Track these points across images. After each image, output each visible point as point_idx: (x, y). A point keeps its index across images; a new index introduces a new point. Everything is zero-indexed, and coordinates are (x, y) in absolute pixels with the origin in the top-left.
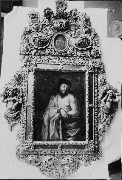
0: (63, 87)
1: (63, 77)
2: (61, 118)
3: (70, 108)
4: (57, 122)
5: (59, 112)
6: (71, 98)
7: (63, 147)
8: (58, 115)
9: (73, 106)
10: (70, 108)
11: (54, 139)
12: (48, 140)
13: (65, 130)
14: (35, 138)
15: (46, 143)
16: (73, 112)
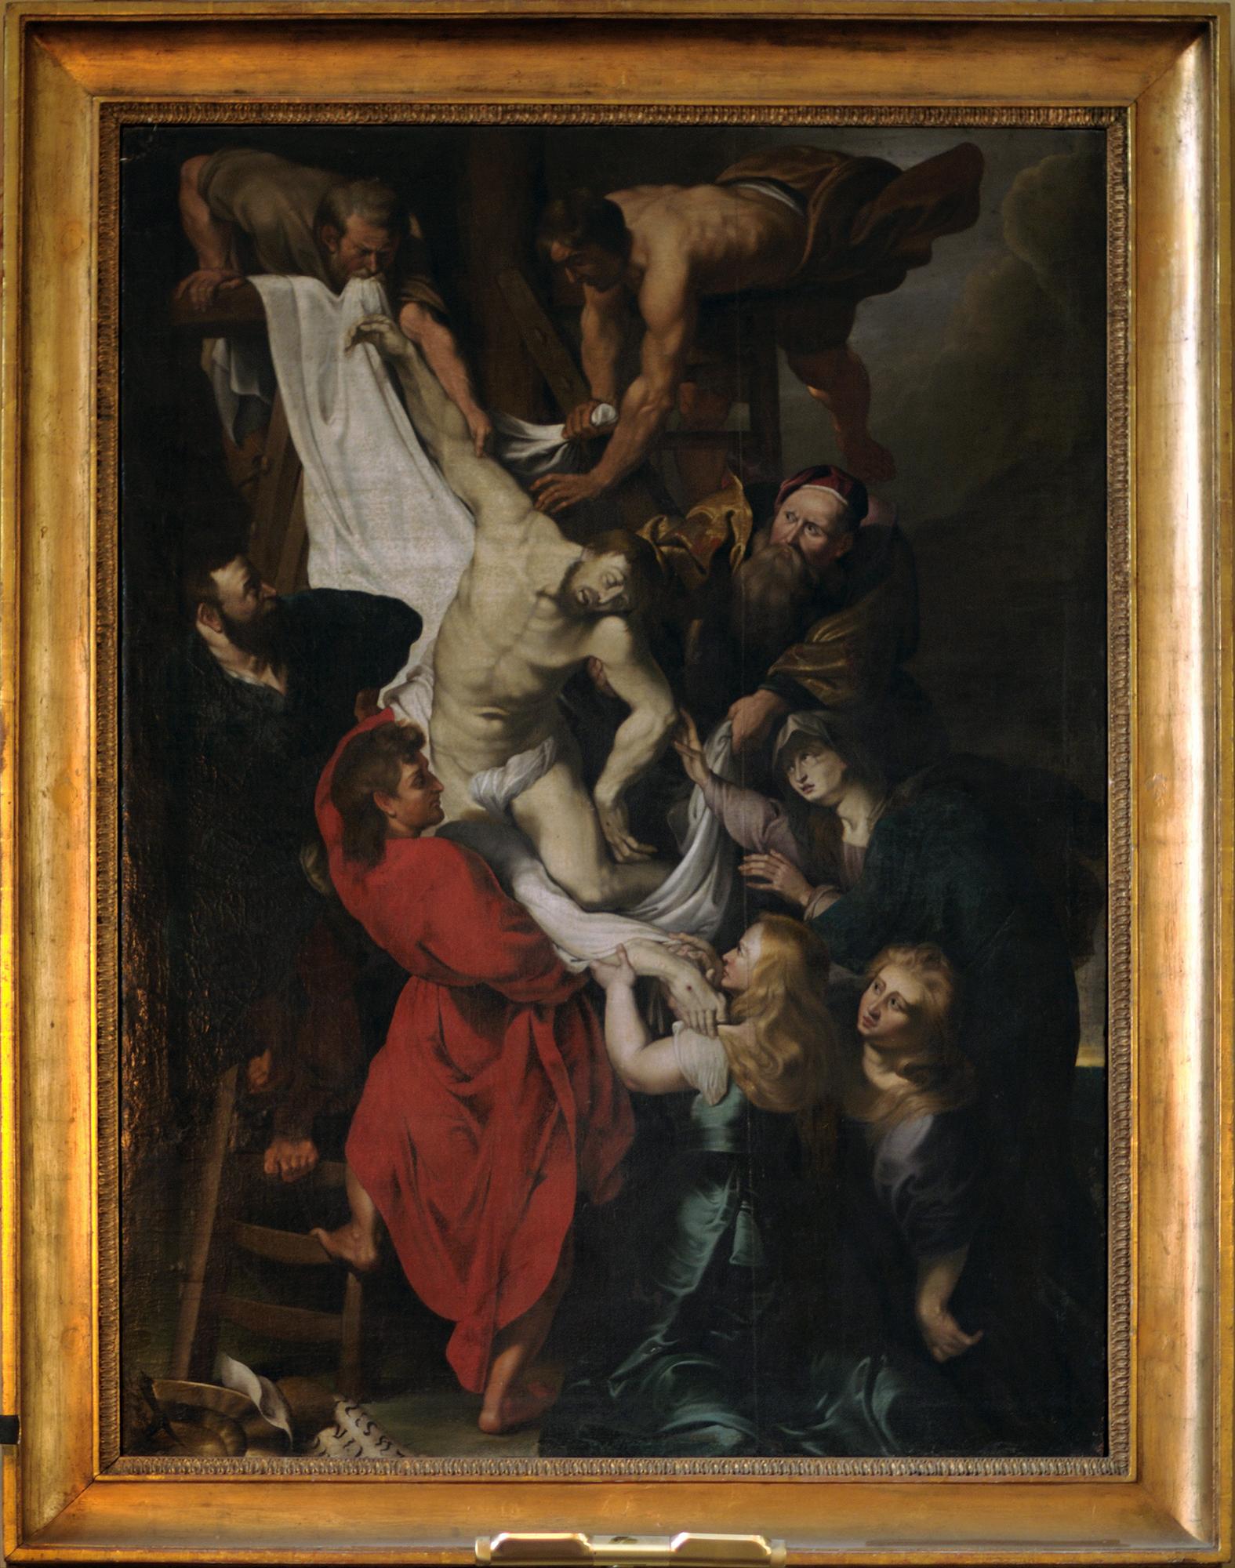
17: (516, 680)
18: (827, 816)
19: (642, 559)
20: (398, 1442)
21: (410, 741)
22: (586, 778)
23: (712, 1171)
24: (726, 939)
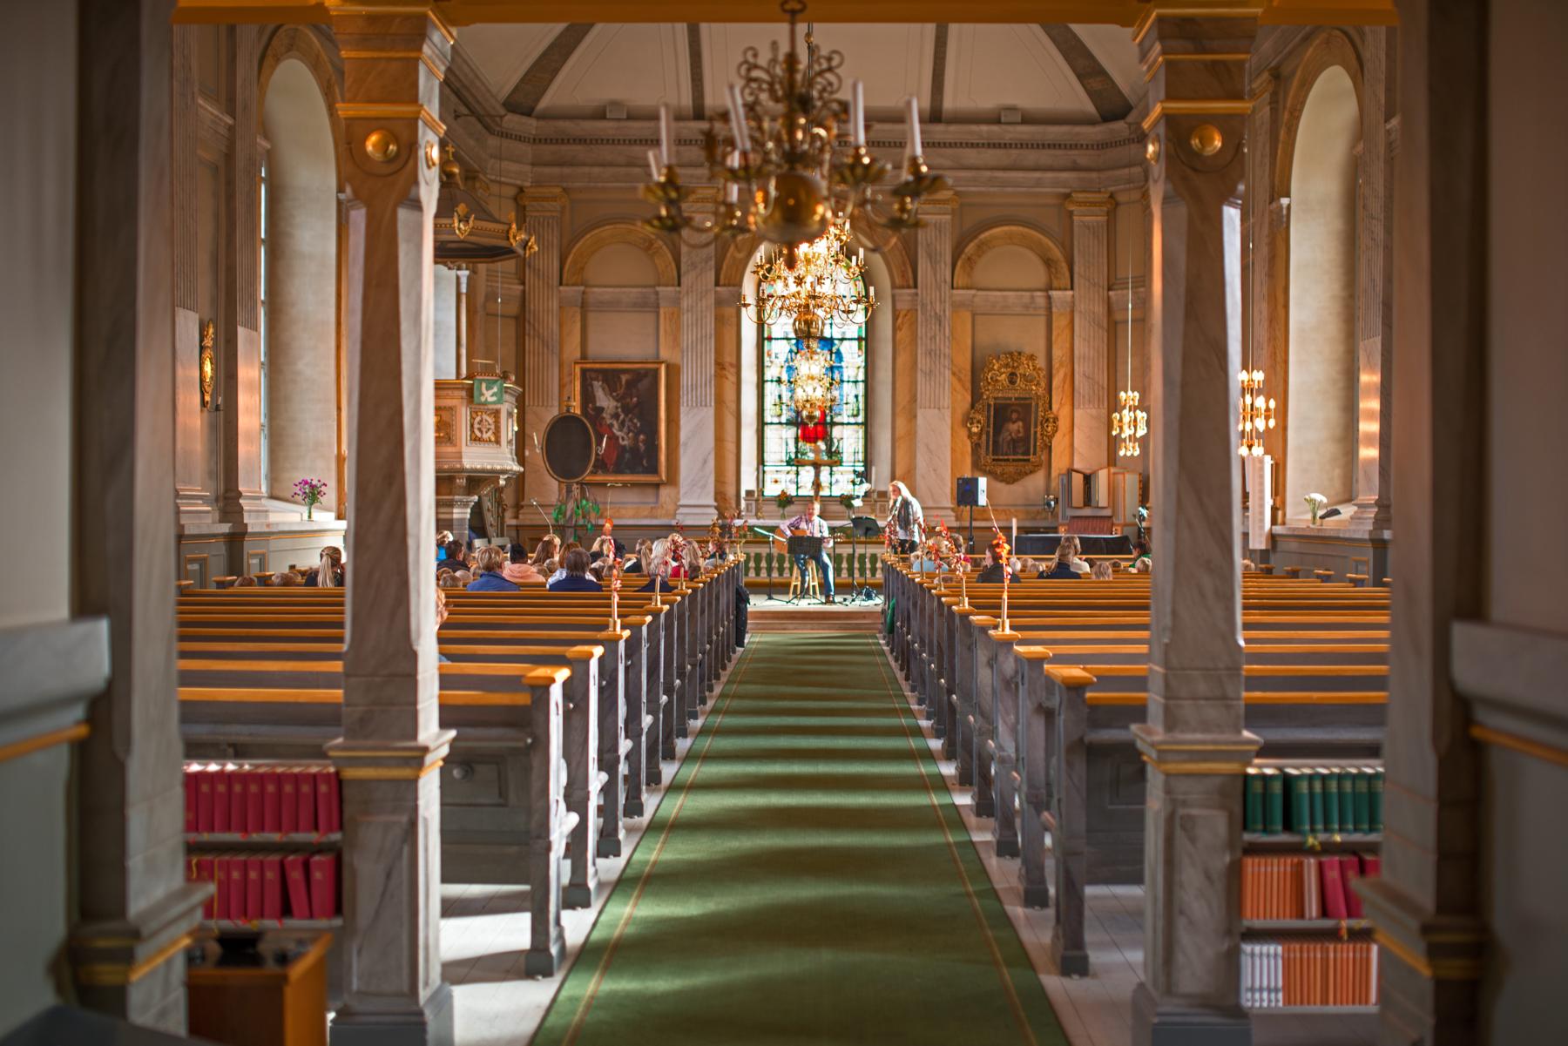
0: (1014, 416)
1: (1013, 408)
2: (1012, 439)
3: (1019, 432)
4: (1009, 443)
5: (1010, 434)
6: (1020, 424)
7: (1014, 460)
8: (1009, 438)
9: (1021, 430)
10: (1019, 432)
12: (1002, 455)
13: (1014, 447)
14: (995, 453)
15: (1001, 457)
16: (1021, 435)
17: (612, 413)
18: (636, 424)
20: (603, 472)
21: (604, 418)
22: (618, 420)
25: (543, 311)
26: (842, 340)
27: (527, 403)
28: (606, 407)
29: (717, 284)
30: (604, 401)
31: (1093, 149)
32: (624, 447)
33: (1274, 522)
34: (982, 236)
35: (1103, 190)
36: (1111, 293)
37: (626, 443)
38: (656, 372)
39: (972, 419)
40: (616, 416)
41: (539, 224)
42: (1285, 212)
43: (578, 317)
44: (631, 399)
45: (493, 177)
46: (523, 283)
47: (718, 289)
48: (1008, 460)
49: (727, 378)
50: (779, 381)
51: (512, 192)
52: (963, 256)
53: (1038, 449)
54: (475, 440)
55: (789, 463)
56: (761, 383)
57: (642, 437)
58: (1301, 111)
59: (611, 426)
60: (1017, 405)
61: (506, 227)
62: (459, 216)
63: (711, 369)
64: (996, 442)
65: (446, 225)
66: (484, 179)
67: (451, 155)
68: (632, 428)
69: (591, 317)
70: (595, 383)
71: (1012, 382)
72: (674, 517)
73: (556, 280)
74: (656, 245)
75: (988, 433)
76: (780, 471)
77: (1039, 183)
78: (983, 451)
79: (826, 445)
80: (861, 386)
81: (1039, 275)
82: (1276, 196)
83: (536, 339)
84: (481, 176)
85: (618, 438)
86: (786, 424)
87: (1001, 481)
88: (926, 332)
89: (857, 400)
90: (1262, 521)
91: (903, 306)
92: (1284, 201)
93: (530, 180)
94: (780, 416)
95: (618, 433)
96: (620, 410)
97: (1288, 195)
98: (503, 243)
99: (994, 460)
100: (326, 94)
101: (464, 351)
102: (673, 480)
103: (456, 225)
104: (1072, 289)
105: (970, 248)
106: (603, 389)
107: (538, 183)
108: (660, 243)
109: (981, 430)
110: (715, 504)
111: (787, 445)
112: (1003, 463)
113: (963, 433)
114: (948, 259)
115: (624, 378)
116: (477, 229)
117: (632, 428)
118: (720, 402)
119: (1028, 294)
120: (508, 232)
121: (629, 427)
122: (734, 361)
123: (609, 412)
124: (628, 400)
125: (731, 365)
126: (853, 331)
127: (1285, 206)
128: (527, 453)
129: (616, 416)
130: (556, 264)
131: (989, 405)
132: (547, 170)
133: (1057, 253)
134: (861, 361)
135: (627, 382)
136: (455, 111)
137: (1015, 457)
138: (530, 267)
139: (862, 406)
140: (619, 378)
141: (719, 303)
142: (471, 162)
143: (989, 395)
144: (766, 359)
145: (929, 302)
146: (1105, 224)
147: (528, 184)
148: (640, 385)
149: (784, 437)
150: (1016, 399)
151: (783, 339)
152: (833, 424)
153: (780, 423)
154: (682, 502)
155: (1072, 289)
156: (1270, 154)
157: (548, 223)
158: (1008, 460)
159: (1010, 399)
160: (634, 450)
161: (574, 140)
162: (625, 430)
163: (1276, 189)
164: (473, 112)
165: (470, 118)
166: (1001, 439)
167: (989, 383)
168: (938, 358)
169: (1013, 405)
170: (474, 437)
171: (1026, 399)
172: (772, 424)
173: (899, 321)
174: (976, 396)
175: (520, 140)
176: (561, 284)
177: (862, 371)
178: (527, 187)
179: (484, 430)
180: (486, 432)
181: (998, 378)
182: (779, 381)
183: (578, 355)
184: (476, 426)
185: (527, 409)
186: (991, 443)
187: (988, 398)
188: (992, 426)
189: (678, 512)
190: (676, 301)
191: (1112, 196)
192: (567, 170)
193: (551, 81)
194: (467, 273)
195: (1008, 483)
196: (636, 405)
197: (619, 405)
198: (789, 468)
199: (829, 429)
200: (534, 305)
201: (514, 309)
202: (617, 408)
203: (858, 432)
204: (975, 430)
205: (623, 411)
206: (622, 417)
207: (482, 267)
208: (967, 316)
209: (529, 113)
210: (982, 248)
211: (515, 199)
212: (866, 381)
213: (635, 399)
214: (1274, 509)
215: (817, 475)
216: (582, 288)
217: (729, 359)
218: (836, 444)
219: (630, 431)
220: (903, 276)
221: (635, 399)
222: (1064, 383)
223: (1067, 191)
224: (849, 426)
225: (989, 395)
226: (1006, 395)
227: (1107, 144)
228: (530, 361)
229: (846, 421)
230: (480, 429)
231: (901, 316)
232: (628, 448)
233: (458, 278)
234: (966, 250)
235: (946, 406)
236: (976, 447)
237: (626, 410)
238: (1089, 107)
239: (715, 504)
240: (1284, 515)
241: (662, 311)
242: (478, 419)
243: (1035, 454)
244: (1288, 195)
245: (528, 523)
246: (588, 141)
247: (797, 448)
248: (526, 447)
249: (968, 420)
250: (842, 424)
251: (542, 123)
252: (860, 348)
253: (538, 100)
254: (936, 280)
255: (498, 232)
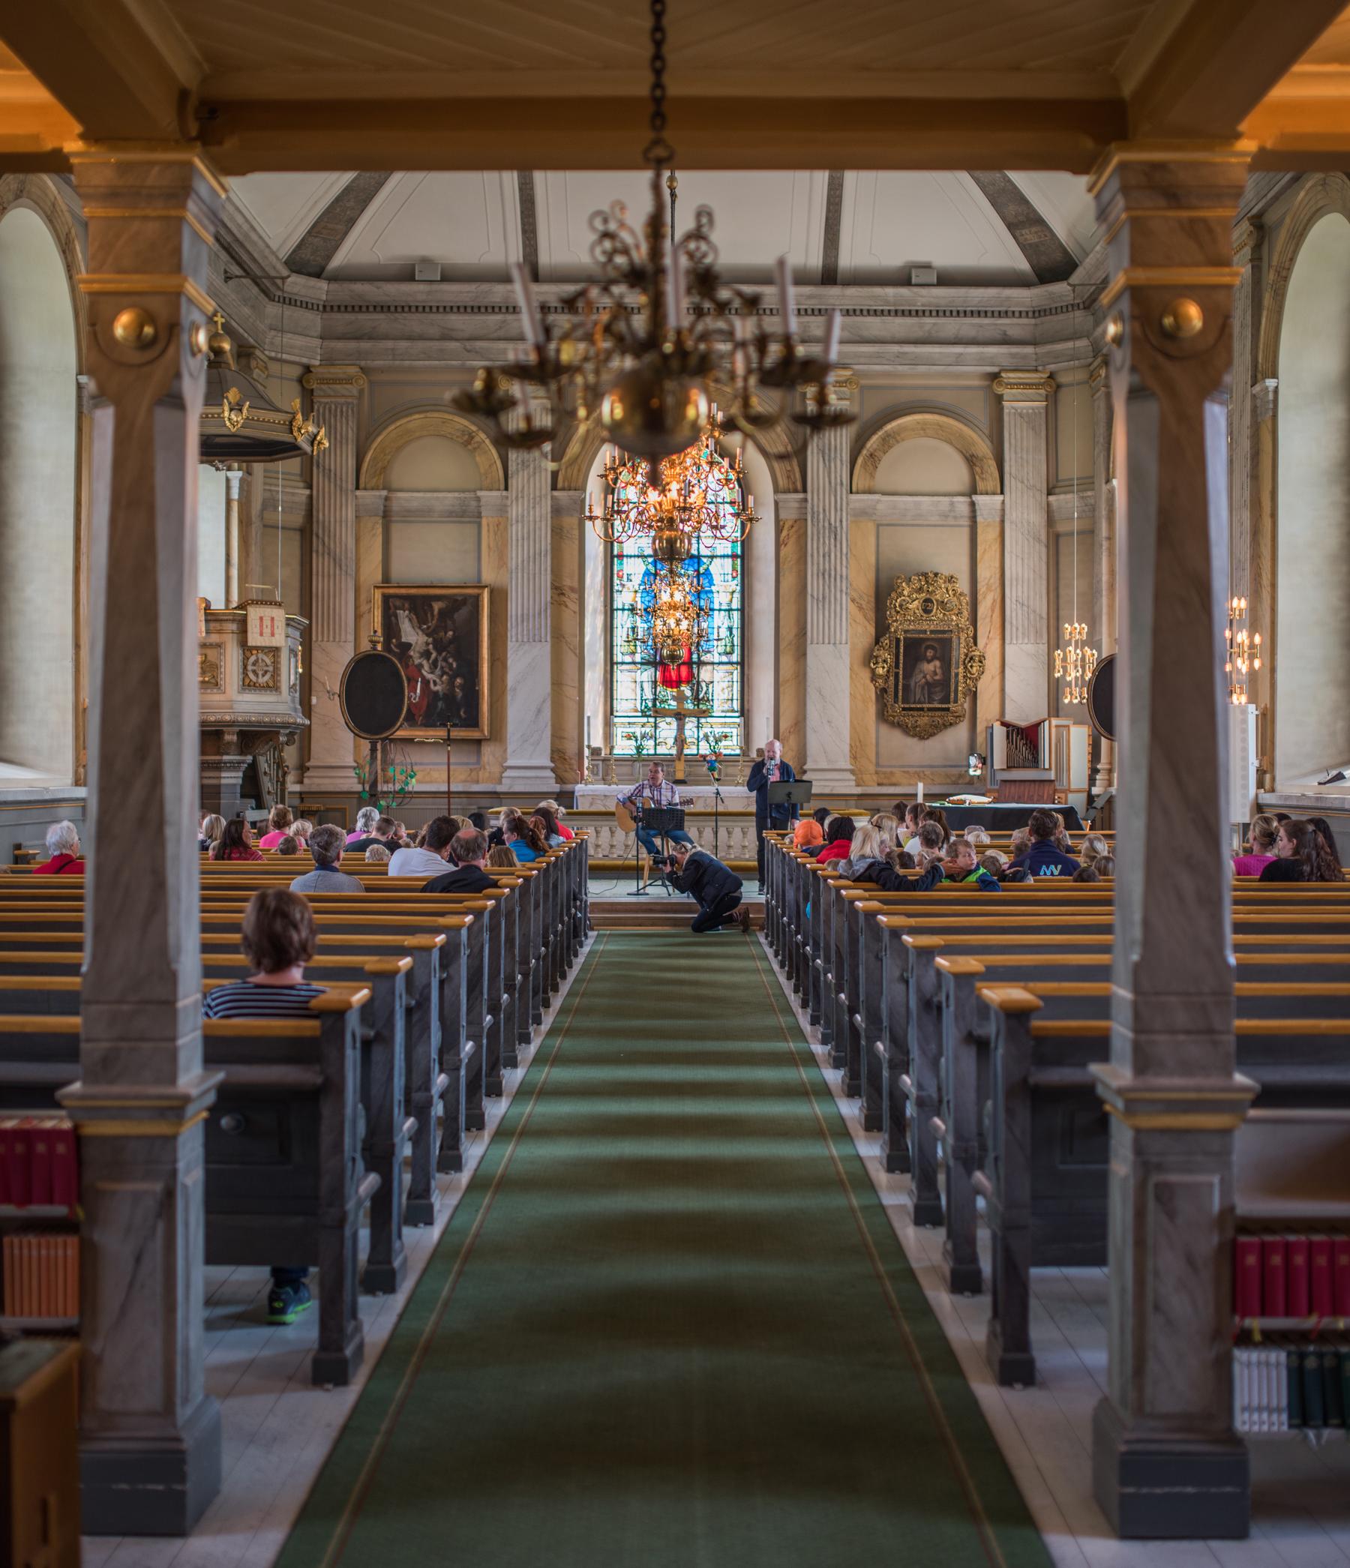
0: (930, 653)
1: (929, 643)
2: (927, 683)
3: (935, 673)
5: (925, 677)
6: (937, 663)
7: (930, 709)
9: (938, 671)
10: (935, 673)
11: (920, 702)
13: (930, 693)
16: (937, 678)
19: (434, 639)
20: (411, 726)
21: (411, 657)
22: (428, 659)
23: (440, 699)
24: (442, 676)
25: (335, 521)
26: (712, 557)
27: (314, 638)
28: (413, 643)
29: (554, 487)
30: (411, 634)
31: (1027, 316)
32: (436, 693)
33: (1260, 784)
34: (889, 427)
35: (1040, 368)
36: (1051, 498)
37: (438, 688)
38: (477, 599)
39: (876, 657)
40: (426, 654)
41: (330, 411)
42: (1271, 396)
43: (379, 530)
44: (446, 633)
45: (273, 354)
46: (310, 487)
47: (556, 493)
48: (922, 709)
49: (566, 606)
50: (633, 610)
51: (296, 371)
52: (864, 452)
53: (960, 695)
54: (249, 685)
55: (644, 715)
56: (610, 611)
57: (459, 681)
58: (1289, 269)
59: (421, 666)
60: (933, 639)
61: (289, 417)
62: (230, 403)
63: (547, 594)
64: (906, 688)
65: (213, 414)
66: (263, 357)
67: (220, 327)
68: (447, 670)
69: (396, 530)
70: (400, 612)
71: (927, 611)
72: (500, 782)
73: (351, 485)
74: (477, 439)
75: (897, 675)
76: (634, 723)
77: (959, 360)
78: (890, 699)
79: (692, 690)
80: (736, 615)
81: (957, 475)
82: (1259, 376)
83: (326, 557)
84: (258, 353)
85: (429, 682)
86: (642, 664)
87: (913, 736)
88: (818, 548)
89: (731, 633)
90: (1245, 787)
91: (789, 514)
92: (1271, 383)
93: (319, 358)
94: (633, 653)
95: (429, 676)
96: (431, 646)
97: (1275, 375)
98: (285, 437)
99: (904, 709)
100: (64, 252)
101: (235, 572)
102: (497, 734)
103: (226, 414)
104: (1002, 493)
105: (873, 442)
106: (410, 620)
107: (329, 360)
108: (483, 436)
109: (888, 671)
110: (553, 765)
111: (642, 690)
112: (915, 713)
113: (866, 675)
114: (846, 456)
115: (437, 606)
116: (253, 419)
117: (447, 670)
118: (558, 636)
119: (947, 499)
120: (291, 423)
121: (442, 668)
122: (576, 585)
123: (417, 649)
124: (442, 634)
125: (572, 589)
126: (724, 548)
127: (1271, 389)
128: (314, 700)
129: (426, 654)
130: (351, 463)
131: (898, 640)
132: (340, 345)
133: (983, 448)
134: (735, 585)
135: (441, 611)
136: (226, 272)
137: (931, 706)
138: (318, 466)
139: (737, 641)
140: (431, 607)
141: (557, 511)
142: (246, 335)
143: (898, 626)
144: (616, 581)
145: (821, 510)
146: (1043, 411)
147: (317, 363)
148: (456, 616)
149: (638, 680)
150: (932, 632)
151: (638, 556)
152: (701, 663)
153: (634, 663)
154: (509, 763)
155: (1002, 493)
156: (1253, 324)
157: (342, 411)
158: (922, 709)
159: (925, 632)
160: (449, 697)
161: (375, 307)
162: (438, 671)
163: (1260, 368)
164: (248, 273)
165: (243, 280)
166: (912, 684)
167: (898, 612)
168: (832, 580)
169: (928, 639)
170: (247, 681)
171: (944, 632)
172: (623, 663)
173: (784, 533)
174: (881, 628)
175: (307, 307)
176: (357, 488)
177: (737, 595)
178: (314, 366)
179: (260, 673)
180: (263, 676)
181: (910, 606)
182: (633, 610)
183: (378, 577)
184: (250, 668)
185: (314, 645)
186: (900, 687)
187: (895, 632)
188: (901, 665)
189: (504, 775)
190: (502, 509)
191: (1051, 376)
192: (365, 345)
193: (346, 233)
194: (240, 474)
195: (922, 738)
196: (451, 642)
197: (430, 640)
198: (645, 720)
199: (695, 671)
200: (324, 515)
201: (298, 519)
202: (427, 644)
203: (732, 673)
204: (880, 671)
205: (435, 648)
206: (434, 655)
207: (258, 468)
208: (871, 527)
209: (318, 275)
210: (887, 443)
211: (300, 381)
212: (742, 610)
213: (451, 633)
214: (1261, 772)
215: (681, 729)
216: (384, 493)
217: (569, 582)
218: (705, 689)
219: (444, 673)
220: (788, 477)
221: (451, 633)
222: (993, 611)
223: (995, 369)
224: (721, 667)
225: (898, 626)
226: (919, 628)
227: (1045, 310)
228: (318, 585)
229: (716, 660)
230: (254, 672)
231: (786, 527)
232: (441, 694)
233: (228, 480)
234: (869, 445)
235: (844, 642)
236: (882, 693)
237: (440, 647)
238: (1022, 264)
239: (553, 765)
240: (1273, 779)
241: (484, 522)
242: (253, 659)
243: (956, 701)
244: (1275, 375)
245: (314, 789)
246: (392, 309)
247: (655, 694)
248: (313, 693)
249: (869, 658)
250: (713, 663)
251: (334, 286)
252: (734, 569)
253: (329, 258)
254: (830, 483)
255: (279, 423)
